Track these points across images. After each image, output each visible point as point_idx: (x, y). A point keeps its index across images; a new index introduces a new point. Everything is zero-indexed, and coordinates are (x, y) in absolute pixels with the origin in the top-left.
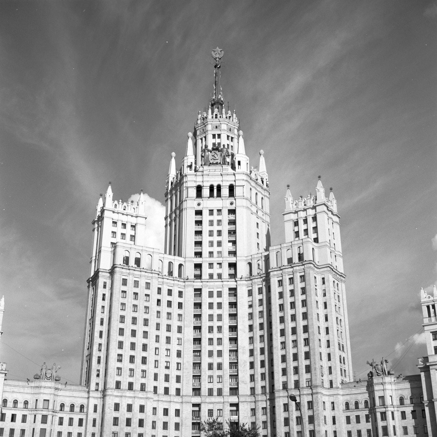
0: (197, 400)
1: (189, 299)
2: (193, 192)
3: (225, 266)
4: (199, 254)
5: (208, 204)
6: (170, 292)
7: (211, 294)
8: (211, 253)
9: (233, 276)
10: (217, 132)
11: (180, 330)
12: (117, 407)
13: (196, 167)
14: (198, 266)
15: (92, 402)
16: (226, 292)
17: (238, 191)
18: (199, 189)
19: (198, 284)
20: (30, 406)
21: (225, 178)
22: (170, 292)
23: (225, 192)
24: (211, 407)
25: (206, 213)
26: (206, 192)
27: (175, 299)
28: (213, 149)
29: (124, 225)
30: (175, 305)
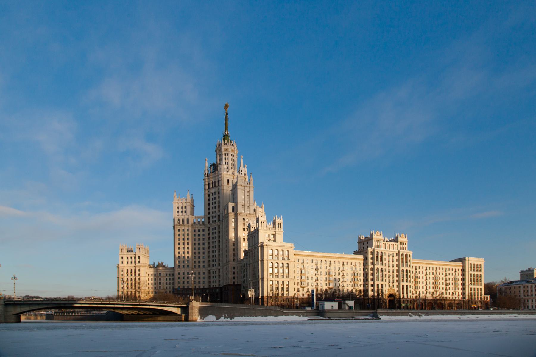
0: (209, 269)
3: (217, 217)
4: (209, 213)
5: (212, 191)
6: (199, 231)
11: (204, 244)
12: (179, 273)
13: (208, 175)
16: (217, 227)
18: (209, 184)
20: (156, 275)
21: (217, 178)
22: (199, 231)
23: (217, 184)
24: (213, 270)
25: (211, 195)
29: (182, 207)
30: (201, 235)
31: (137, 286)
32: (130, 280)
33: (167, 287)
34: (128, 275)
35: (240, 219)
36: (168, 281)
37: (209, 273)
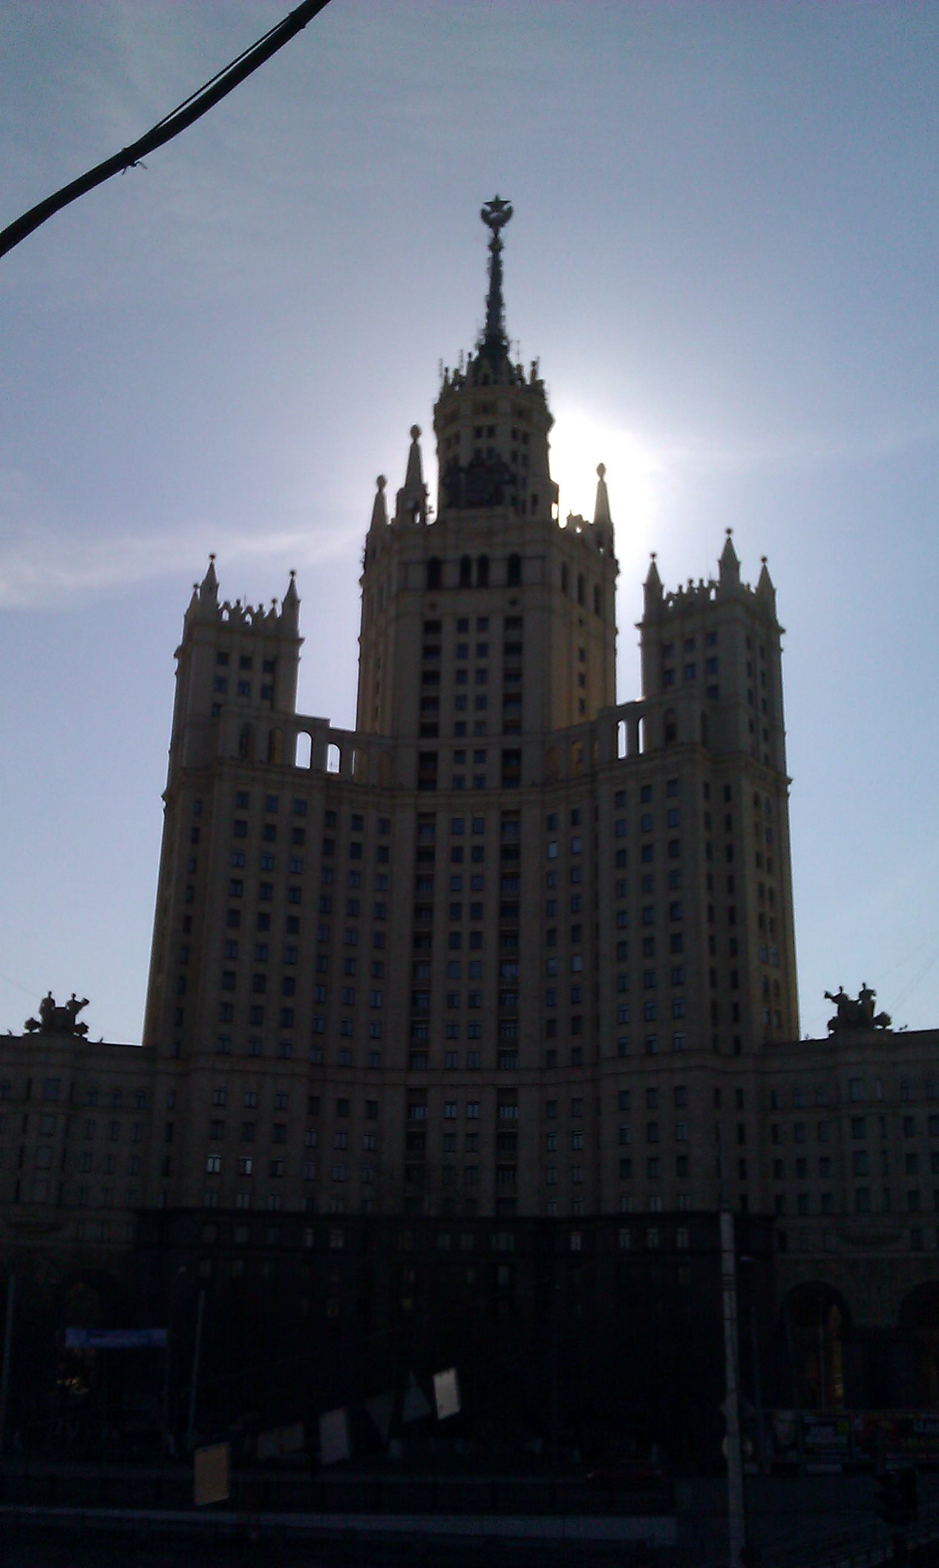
0: (417, 1079)
2: (418, 576)
3: (494, 757)
7: (457, 827)
9: (510, 779)
10: (485, 421)
14: (428, 760)
16: (493, 820)
22: (357, 822)
23: (498, 572)
25: (448, 626)
26: (451, 574)
28: (472, 465)
29: (246, 663)
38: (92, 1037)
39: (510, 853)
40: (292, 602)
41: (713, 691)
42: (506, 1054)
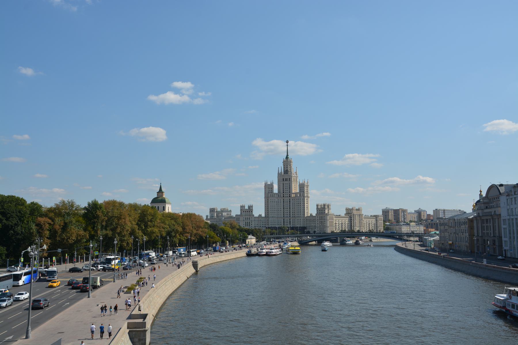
1: (282, 201)
2: (282, 180)
3: (288, 195)
4: (283, 192)
7: (286, 200)
8: (286, 192)
9: (290, 196)
15: (267, 219)
17: (291, 180)
18: (283, 179)
19: (284, 198)
23: (288, 180)
25: (285, 184)
26: (285, 180)
27: (280, 201)
29: (270, 188)
31: (251, 225)
32: (247, 223)
33: (263, 226)
34: (246, 220)
35: (305, 199)
36: (263, 223)
37: (284, 220)
38: (262, 216)
39: (290, 202)
40: (273, 183)
41: (303, 192)
42: (290, 217)
